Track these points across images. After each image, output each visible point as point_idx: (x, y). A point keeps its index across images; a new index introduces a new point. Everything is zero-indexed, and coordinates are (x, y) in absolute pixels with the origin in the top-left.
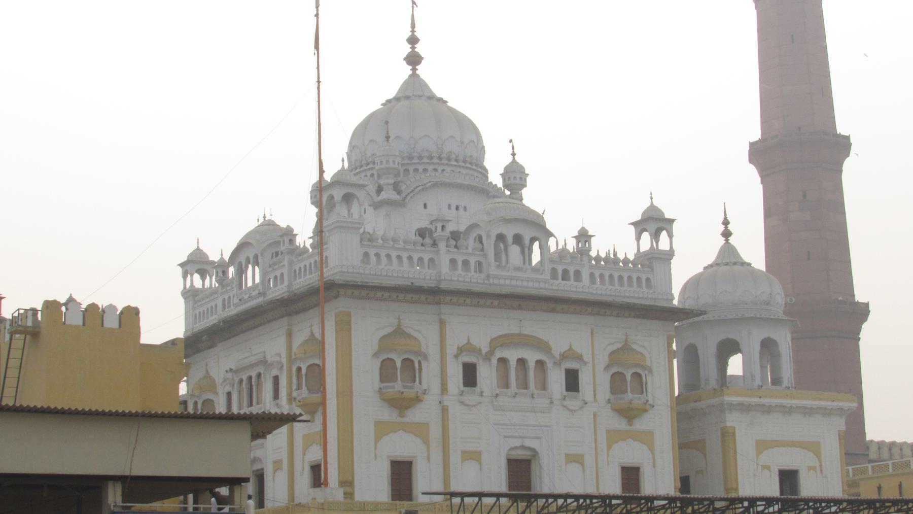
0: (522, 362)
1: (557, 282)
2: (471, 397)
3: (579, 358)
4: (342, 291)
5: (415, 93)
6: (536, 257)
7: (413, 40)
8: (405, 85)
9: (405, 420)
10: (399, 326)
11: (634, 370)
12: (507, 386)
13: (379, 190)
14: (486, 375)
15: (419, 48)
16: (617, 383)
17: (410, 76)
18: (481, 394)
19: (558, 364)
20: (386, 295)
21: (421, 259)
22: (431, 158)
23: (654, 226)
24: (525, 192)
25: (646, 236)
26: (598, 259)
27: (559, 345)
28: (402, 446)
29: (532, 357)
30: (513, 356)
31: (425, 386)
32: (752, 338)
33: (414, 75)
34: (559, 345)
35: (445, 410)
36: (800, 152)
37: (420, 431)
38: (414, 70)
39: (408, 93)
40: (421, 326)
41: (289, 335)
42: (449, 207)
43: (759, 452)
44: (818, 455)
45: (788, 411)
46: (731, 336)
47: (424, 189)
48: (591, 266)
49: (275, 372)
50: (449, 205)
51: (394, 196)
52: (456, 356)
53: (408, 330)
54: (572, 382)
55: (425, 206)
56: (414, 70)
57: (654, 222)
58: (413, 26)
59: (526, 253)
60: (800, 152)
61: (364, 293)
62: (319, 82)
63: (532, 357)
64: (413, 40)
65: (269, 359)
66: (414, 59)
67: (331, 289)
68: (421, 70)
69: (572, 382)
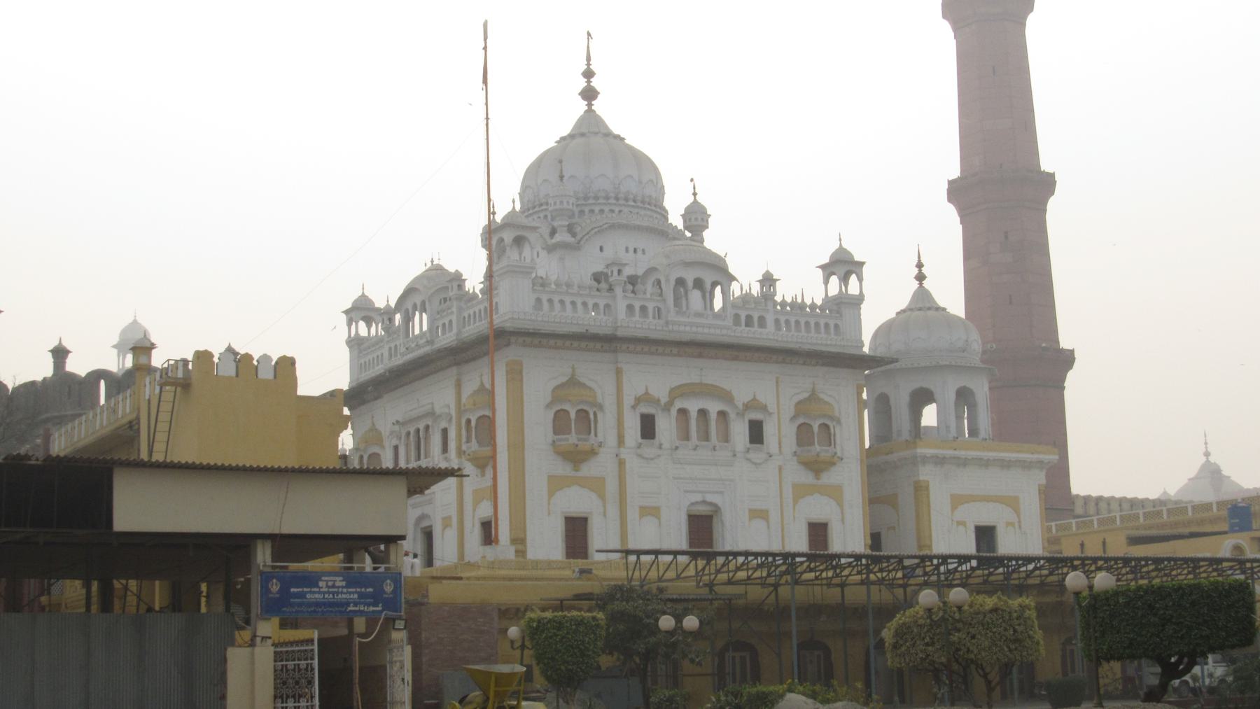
0: (703, 413)
1: (739, 329)
2: (649, 450)
3: (764, 408)
4: (513, 339)
5: (590, 130)
6: (718, 303)
7: (589, 74)
9: (580, 474)
10: (573, 375)
11: (821, 421)
12: (686, 437)
13: (553, 232)
14: (666, 426)
15: (595, 82)
16: (804, 435)
18: (660, 446)
19: (741, 415)
20: (560, 343)
21: (596, 306)
22: (607, 198)
23: (843, 270)
24: (706, 234)
25: (834, 280)
26: (783, 304)
27: (742, 395)
28: (577, 501)
29: (713, 407)
30: (693, 406)
31: (600, 438)
32: (948, 388)
33: (590, 111)
34: (742, 395)
35: (621, 464)
36: (1002, 191)
37: (596, 486)
38: (590, 105)
39: (584, 130)
40: (597, 375)
41: (458, 385)
42: (627, 250)
43: (954, 508)
44: (1017, 511)
45: (985, 464)
46: (925, 385)
47: (601, 231)
48: (777, 312)
49: (443, 424)
51: (567, 238)
52: (634, 407)
53: (582, 380)
54: (756, 433)
55: (601, 249)
56: (590, 105)
57: (843, 265)
58: (589, 59)
59: (708, 298)
60: (1002, 191)
61: (536, 341)
62: (487, 119)
63: (713, 407)
64: (589, 74)
65: (438, 411)
66: (589, 94)
67: (501, 337)
68: (597, 105)
69: (756, 433)
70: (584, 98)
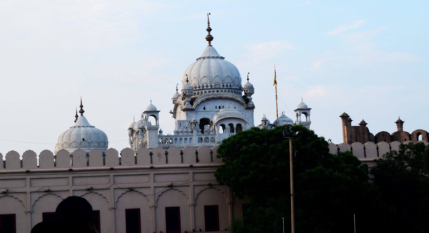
7: (209, 30)
15: (212, 33)
38: (210, 43)
50: (216, 107)
55: (204, 109)
56: (210, 43)
58: (209, 24)
64: (209, 30)
66: (210, 39)
70: (207, 40)
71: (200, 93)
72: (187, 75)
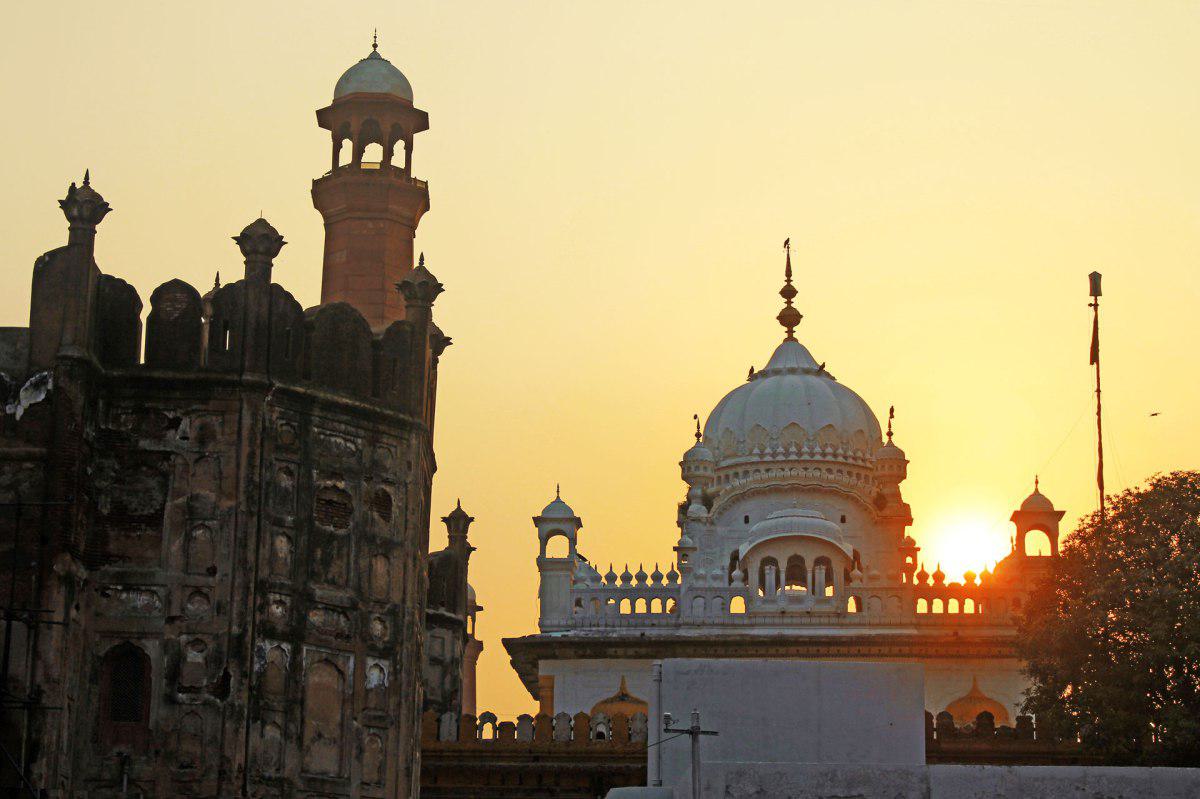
5: (792, 362)
7: (789, 292)
8: (778, 353)
15: (797, 303)
17: (786, 340)
33: (790, 339)
38: (790, 332)
39: (779, 366)
47: (743, 497)
55: (747, 520)
56: (790, 332)
58: (789, 273)
64: (789, 292)
66: (789, 318)
68: (799, 332)
70: (783, 323)
71: (741, 474)
72: (696, 417)
